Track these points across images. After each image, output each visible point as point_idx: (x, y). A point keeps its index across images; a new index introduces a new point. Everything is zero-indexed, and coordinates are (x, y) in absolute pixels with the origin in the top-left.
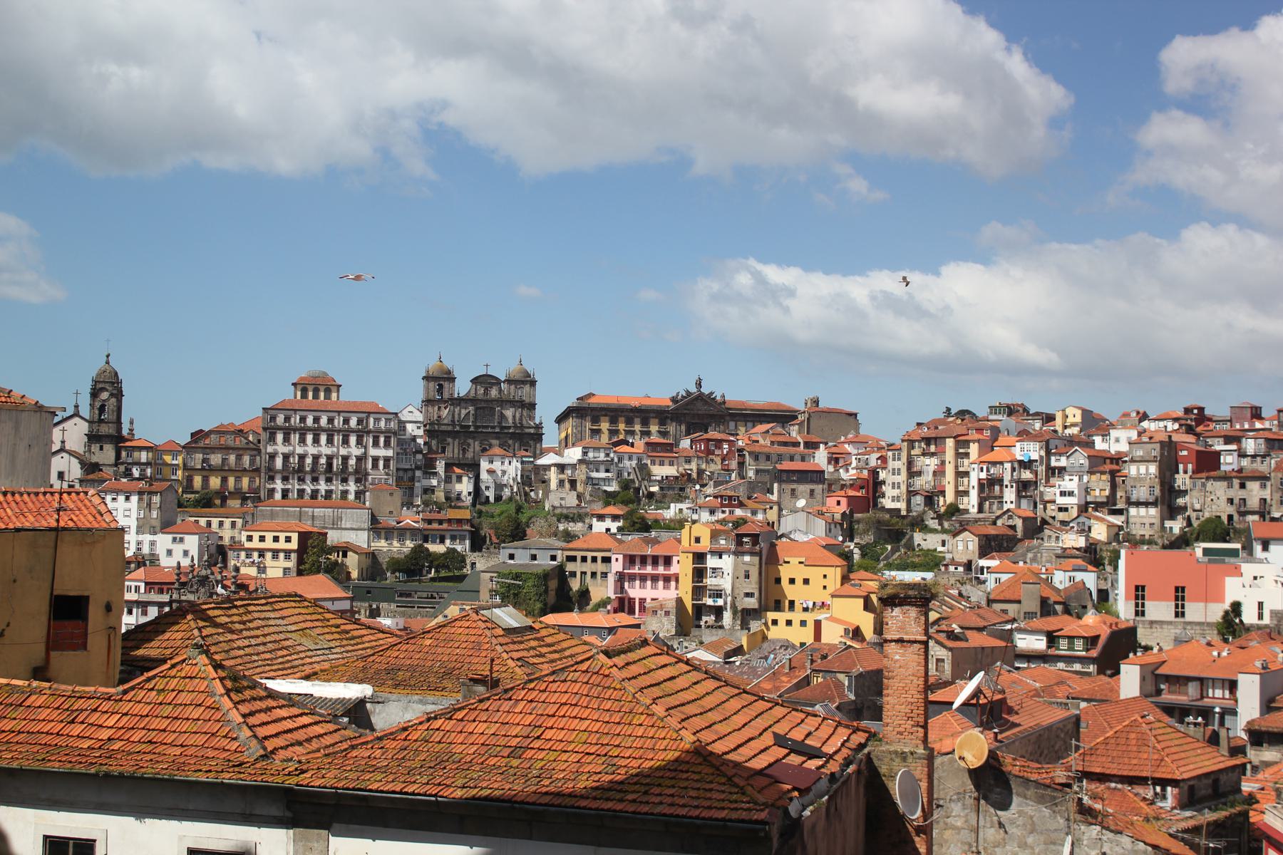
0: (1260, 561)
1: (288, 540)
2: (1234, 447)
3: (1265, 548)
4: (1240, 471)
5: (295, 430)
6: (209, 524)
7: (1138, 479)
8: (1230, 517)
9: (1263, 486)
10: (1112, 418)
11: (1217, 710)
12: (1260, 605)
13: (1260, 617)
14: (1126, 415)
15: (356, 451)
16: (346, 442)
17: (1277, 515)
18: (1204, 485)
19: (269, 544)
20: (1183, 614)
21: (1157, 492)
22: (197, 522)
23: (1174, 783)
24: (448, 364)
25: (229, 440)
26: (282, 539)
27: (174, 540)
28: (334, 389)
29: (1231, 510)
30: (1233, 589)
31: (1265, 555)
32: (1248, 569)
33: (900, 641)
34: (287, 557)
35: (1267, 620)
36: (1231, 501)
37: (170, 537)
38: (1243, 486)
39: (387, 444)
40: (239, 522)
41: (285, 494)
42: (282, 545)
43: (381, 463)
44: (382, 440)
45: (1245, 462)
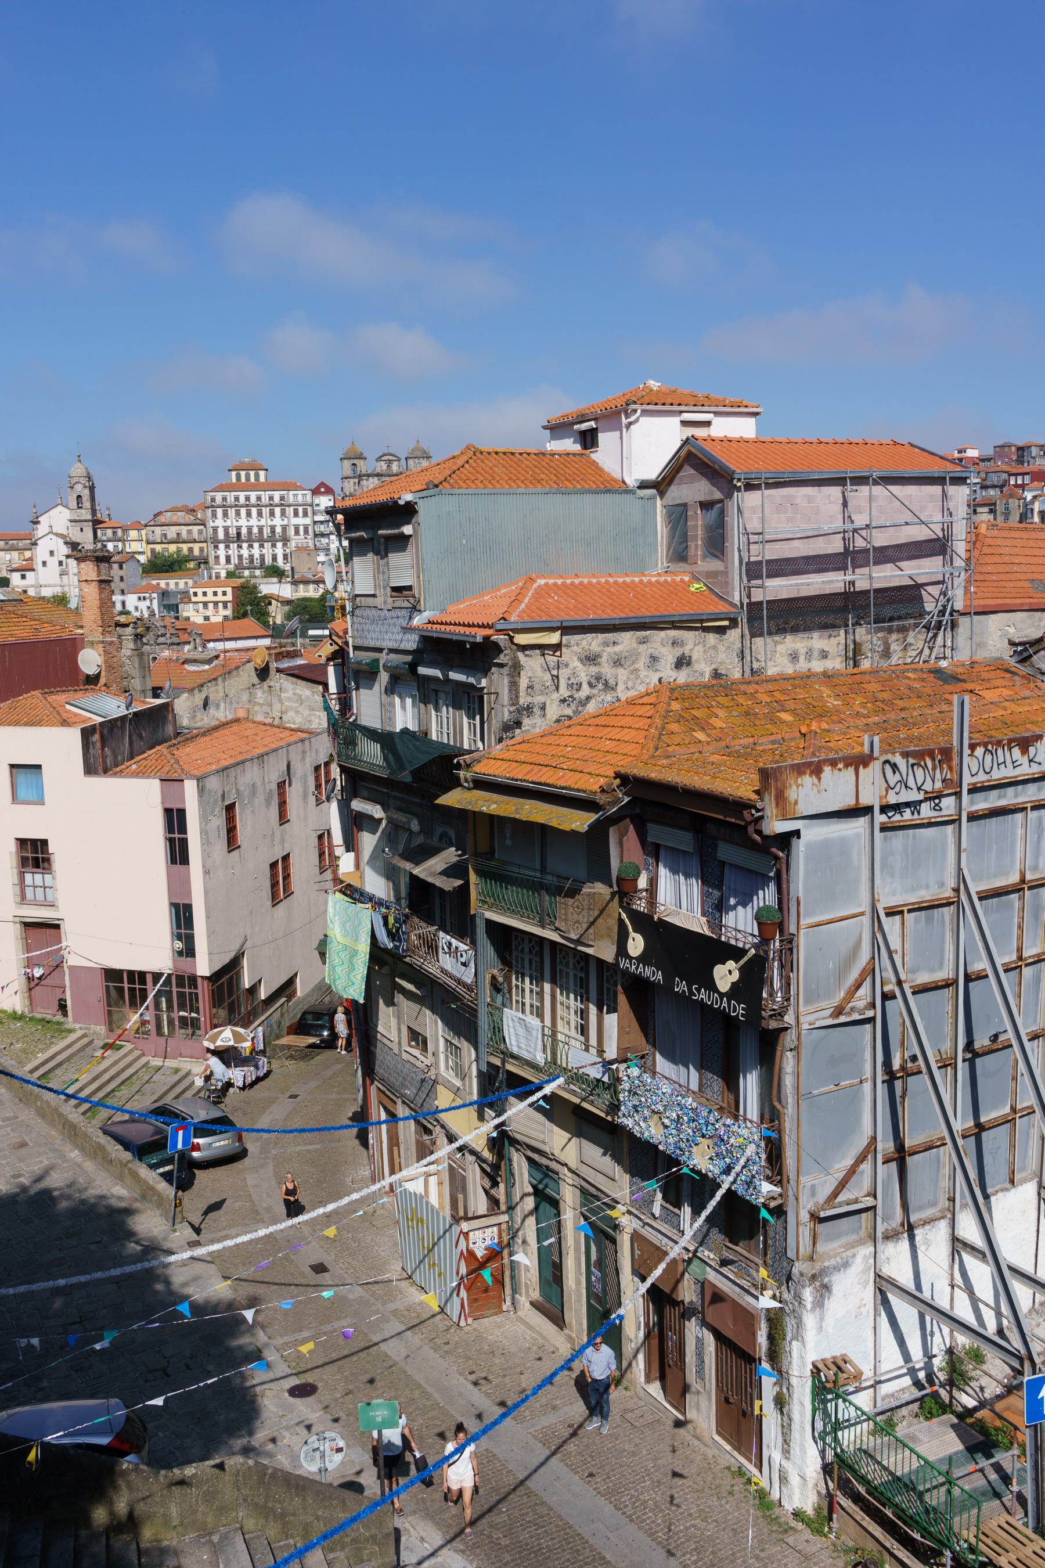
1: (224, 593)
5: (231, 507)
6: (167, 584)
15: (278, 522)
16: (272, 514)
19: (210, 597)
22: (158, 584)
24: (360, 448)
25: (181, 517)
26: (220, 593)
27: (139, 598)
28: (262, 473)
33: (86, 581)
34: (225, 607)
37: (135, 596)
39: (305, 514)
40: (190, 582)
41: (228, 560)
42: (220, 598)
43: (301, 529)
44: (300, 509)
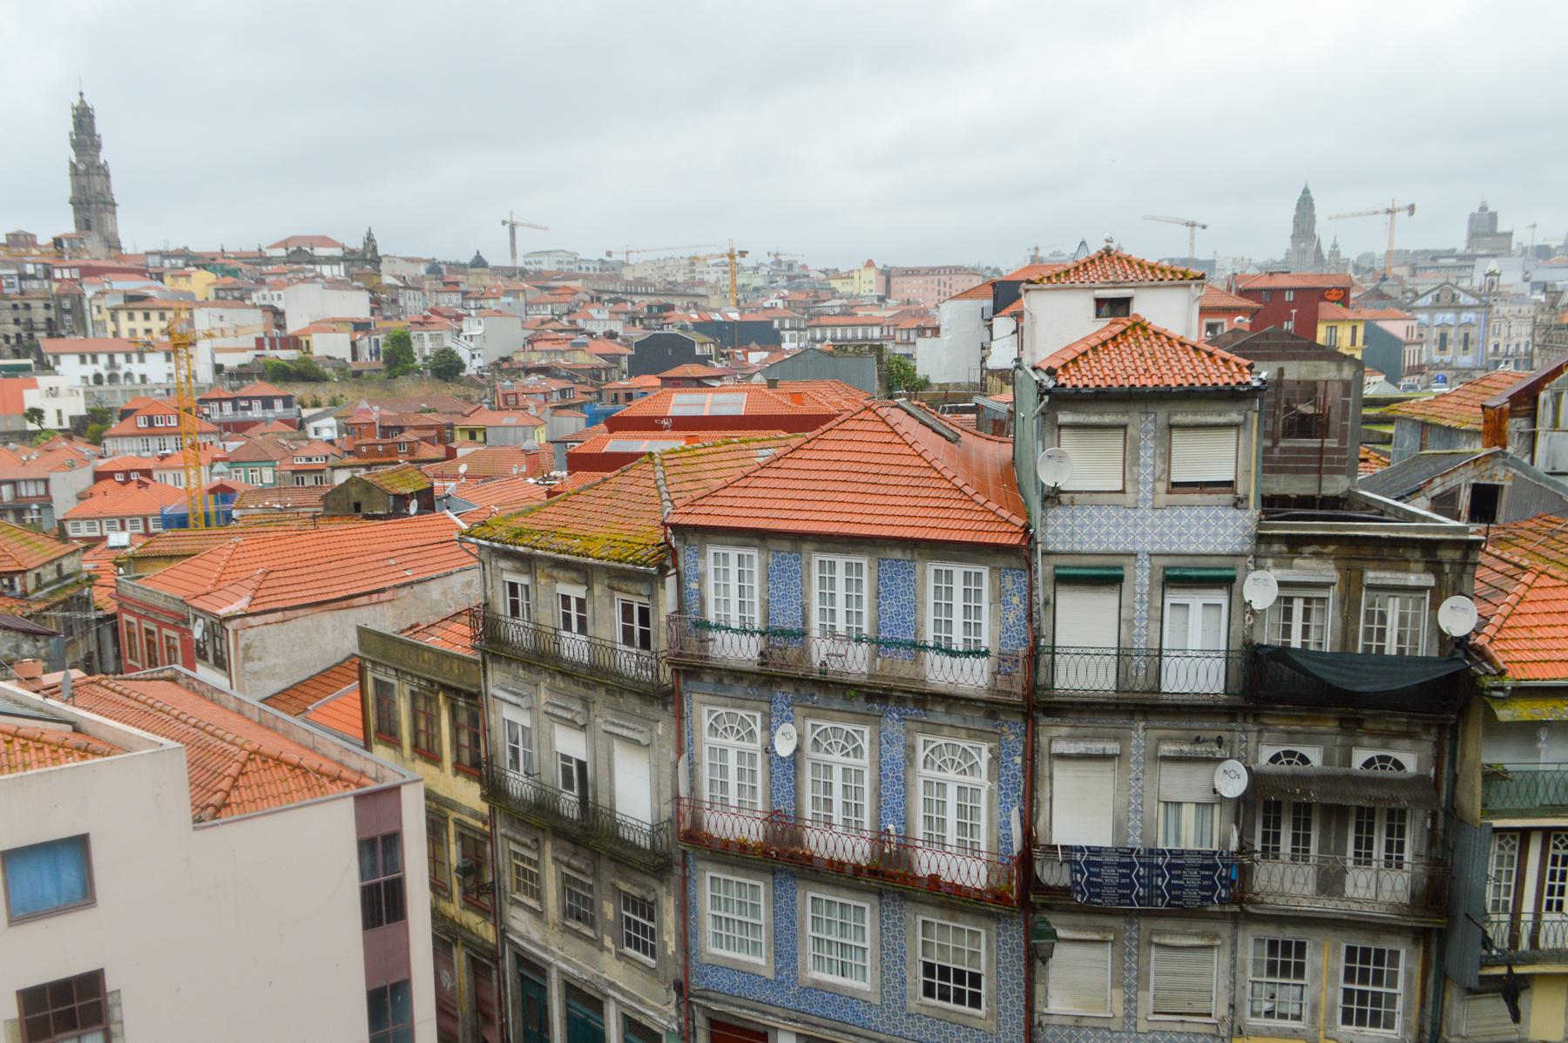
2: (14, 272)
3: (57, 362)
8: (18, 336)
12: (59, 413)
13: (60, 422)
23: (23, 572)
30: (32, 399)
32: (44, 381)
35: (66, 425)
36: (17, 321)
38: (28, 307)
45: (26, 285)
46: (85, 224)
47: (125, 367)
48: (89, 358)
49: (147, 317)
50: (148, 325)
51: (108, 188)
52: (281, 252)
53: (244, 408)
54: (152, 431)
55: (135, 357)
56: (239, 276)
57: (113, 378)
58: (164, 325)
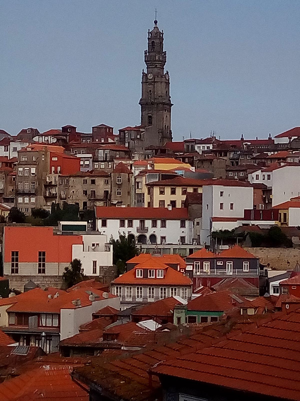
0: (100, 234)
2: (90, 155)
4: (91, 172)
7: (23, 177)
8: (85, 204)
9: (107, 183)
10: (14, 132)
11: (44, 334)
12: (95, 263)
13: (95, 272)
14: (24, 131)
17: (115, 202)
18: (68, 181)
20: (44, 271)
21: (37, 185)
29: (85, 199)
30: (77, 252)
31: (104, 229)
35: (98, 274)
36: (85, 192)
38: (93, 182)
46: (147, 120)
47: (151, 231)
48: (126, 222)
49: (173, 192)
50: (173, 198)
51: (167, 92)
52: (285, 140)
53: (219, 267)
54: (146, 282)
55: (159, 222)
56: (238, 159)
57: (142, 238)
58: (184, 198)
